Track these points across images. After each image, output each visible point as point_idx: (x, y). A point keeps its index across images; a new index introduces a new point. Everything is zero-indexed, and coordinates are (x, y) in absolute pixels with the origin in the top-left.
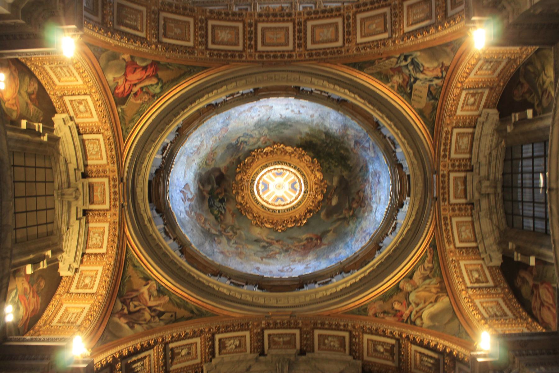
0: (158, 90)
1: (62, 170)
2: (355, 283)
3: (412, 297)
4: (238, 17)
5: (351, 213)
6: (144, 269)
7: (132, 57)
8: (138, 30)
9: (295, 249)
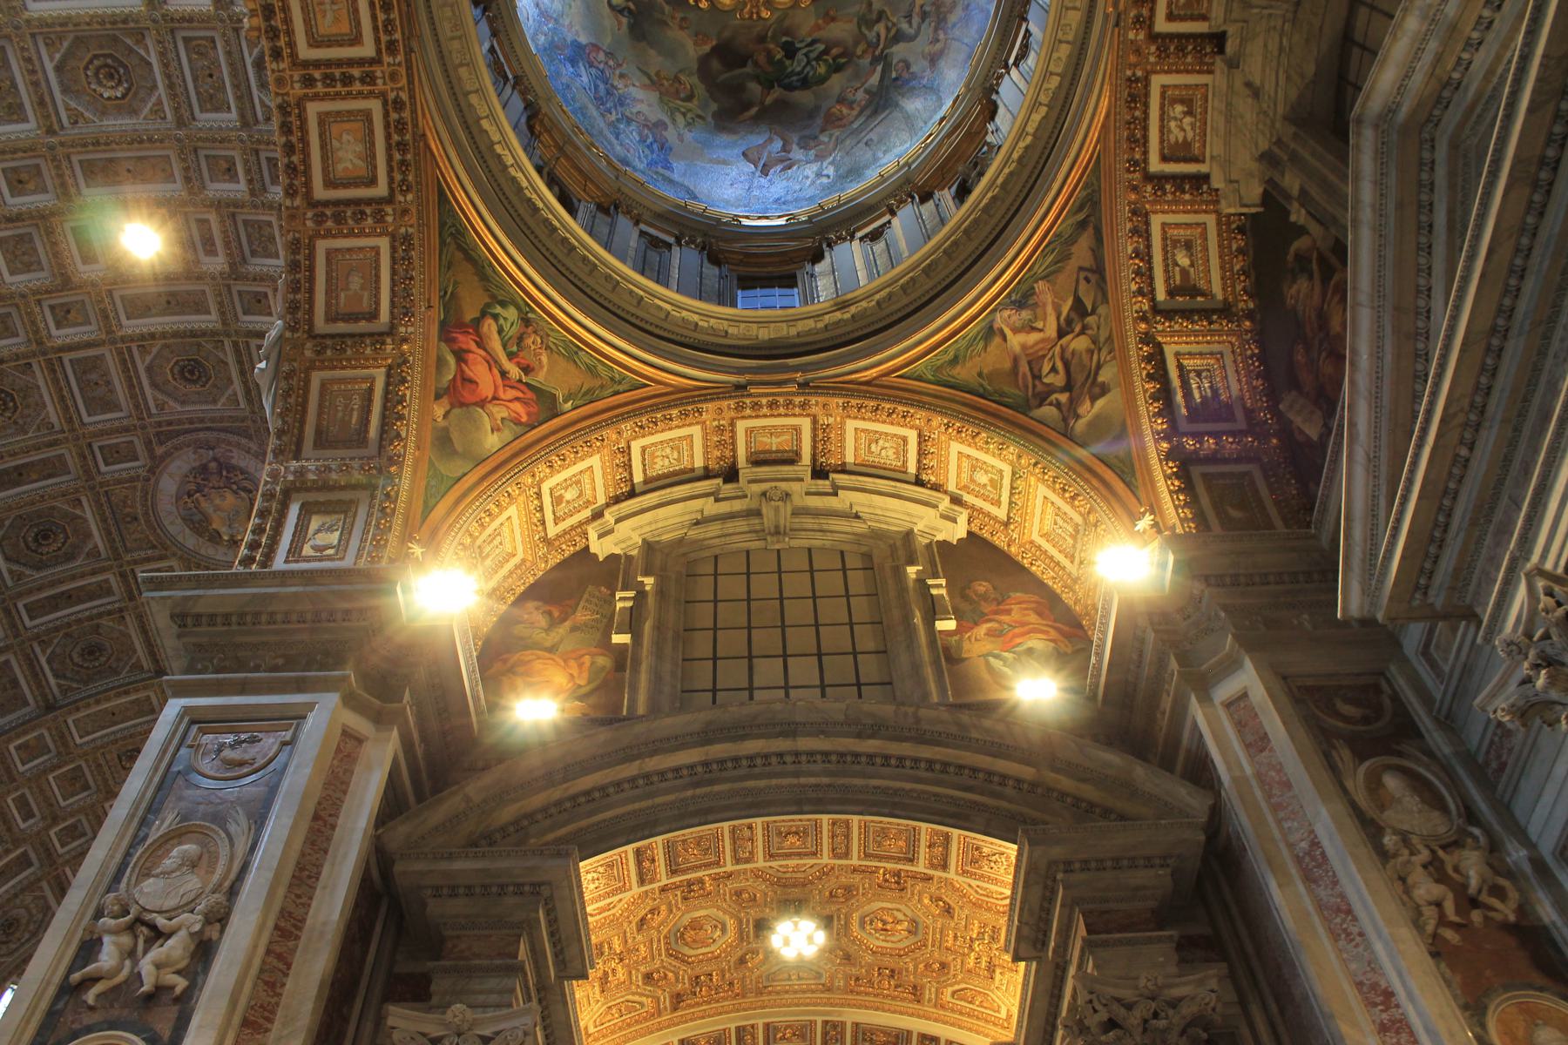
0: (511, 314)
1: (719, 533)
4: (292, 116)
6: (964, 338)
7: (438, 397)
8: (371, 390)
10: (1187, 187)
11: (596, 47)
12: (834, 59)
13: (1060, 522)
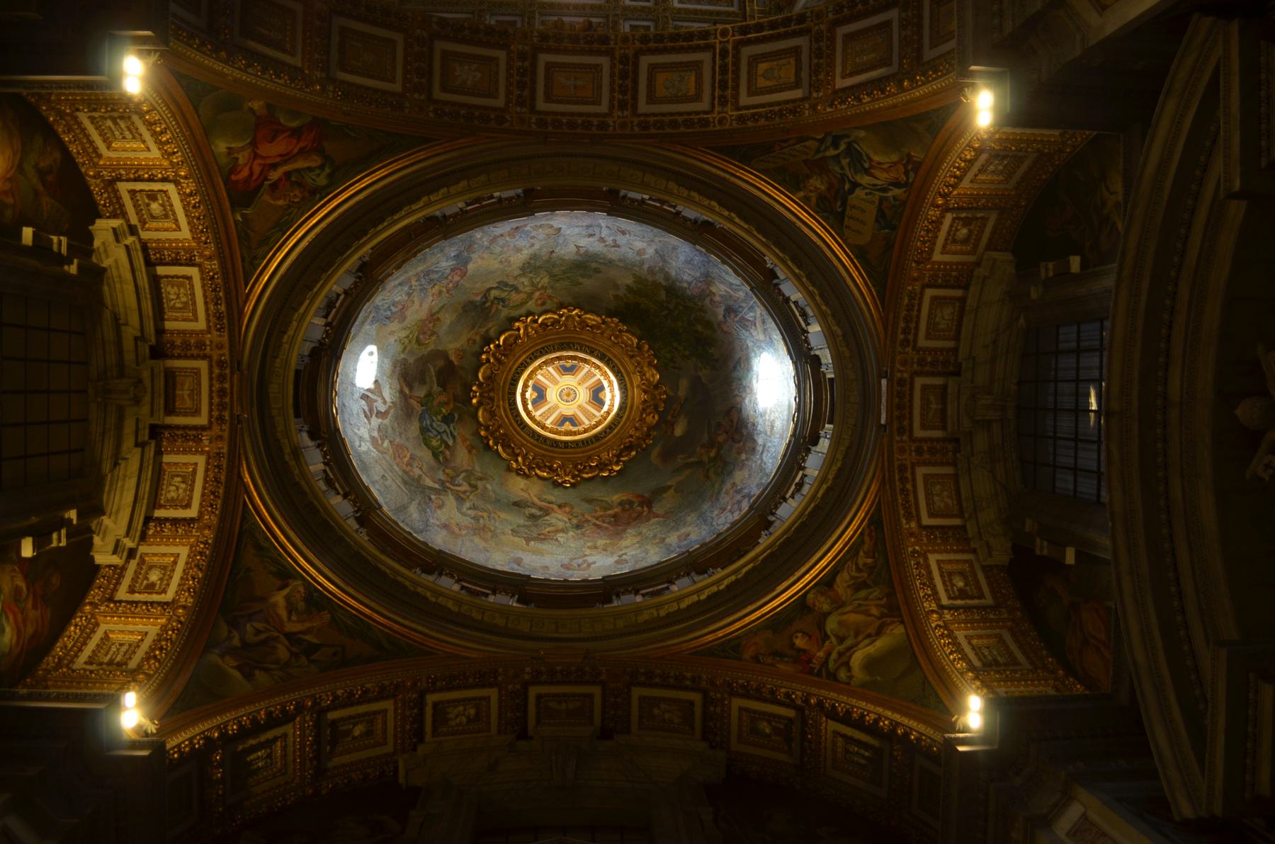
0: (322, 181)
2: (719, 592)
3: (831, 624)
5: (712, 454)
8: (284, 51)
9: (598, 522)
10: (415, 726)
11: (464, 274)
12: (441, 452)
13: (124, 649)
